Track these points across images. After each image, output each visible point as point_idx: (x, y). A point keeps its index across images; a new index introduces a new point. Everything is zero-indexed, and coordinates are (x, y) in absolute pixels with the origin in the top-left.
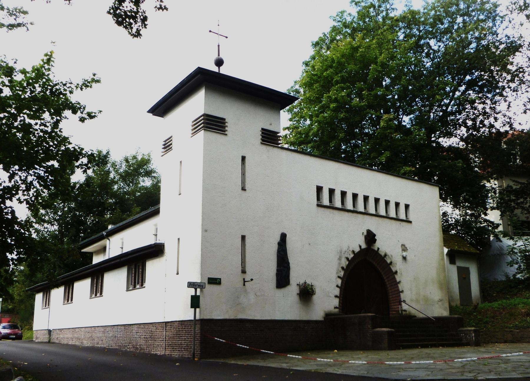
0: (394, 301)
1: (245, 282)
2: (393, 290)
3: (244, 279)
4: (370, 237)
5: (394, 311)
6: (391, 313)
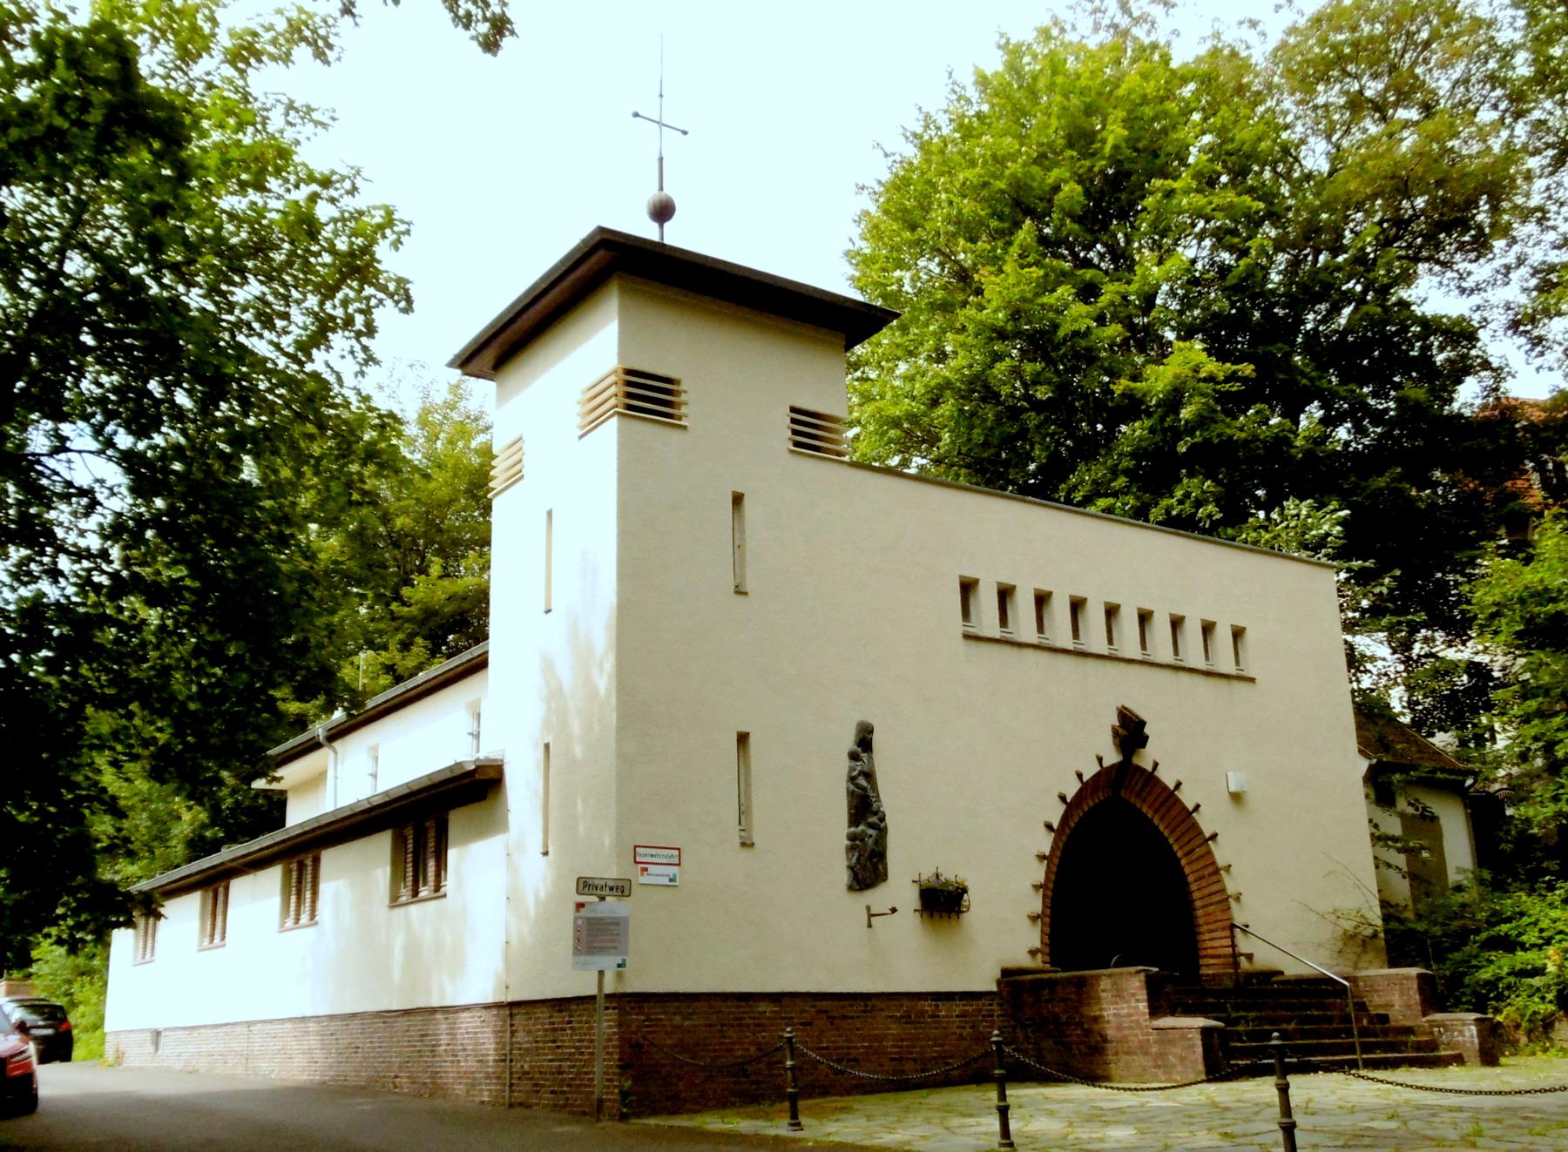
0: (1212, 927)
1: (871, 916)
2: (1207, 891)
3: (868, 908)
4: (1131, 732)
5: (1212, 957)
6: (1202, 962)
